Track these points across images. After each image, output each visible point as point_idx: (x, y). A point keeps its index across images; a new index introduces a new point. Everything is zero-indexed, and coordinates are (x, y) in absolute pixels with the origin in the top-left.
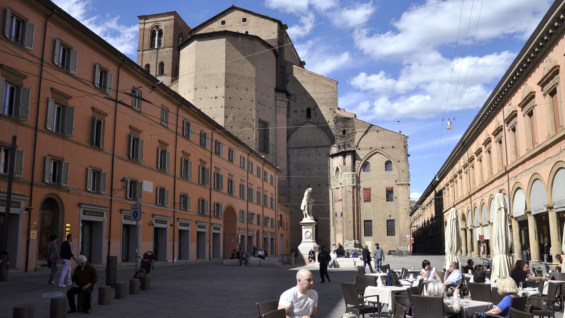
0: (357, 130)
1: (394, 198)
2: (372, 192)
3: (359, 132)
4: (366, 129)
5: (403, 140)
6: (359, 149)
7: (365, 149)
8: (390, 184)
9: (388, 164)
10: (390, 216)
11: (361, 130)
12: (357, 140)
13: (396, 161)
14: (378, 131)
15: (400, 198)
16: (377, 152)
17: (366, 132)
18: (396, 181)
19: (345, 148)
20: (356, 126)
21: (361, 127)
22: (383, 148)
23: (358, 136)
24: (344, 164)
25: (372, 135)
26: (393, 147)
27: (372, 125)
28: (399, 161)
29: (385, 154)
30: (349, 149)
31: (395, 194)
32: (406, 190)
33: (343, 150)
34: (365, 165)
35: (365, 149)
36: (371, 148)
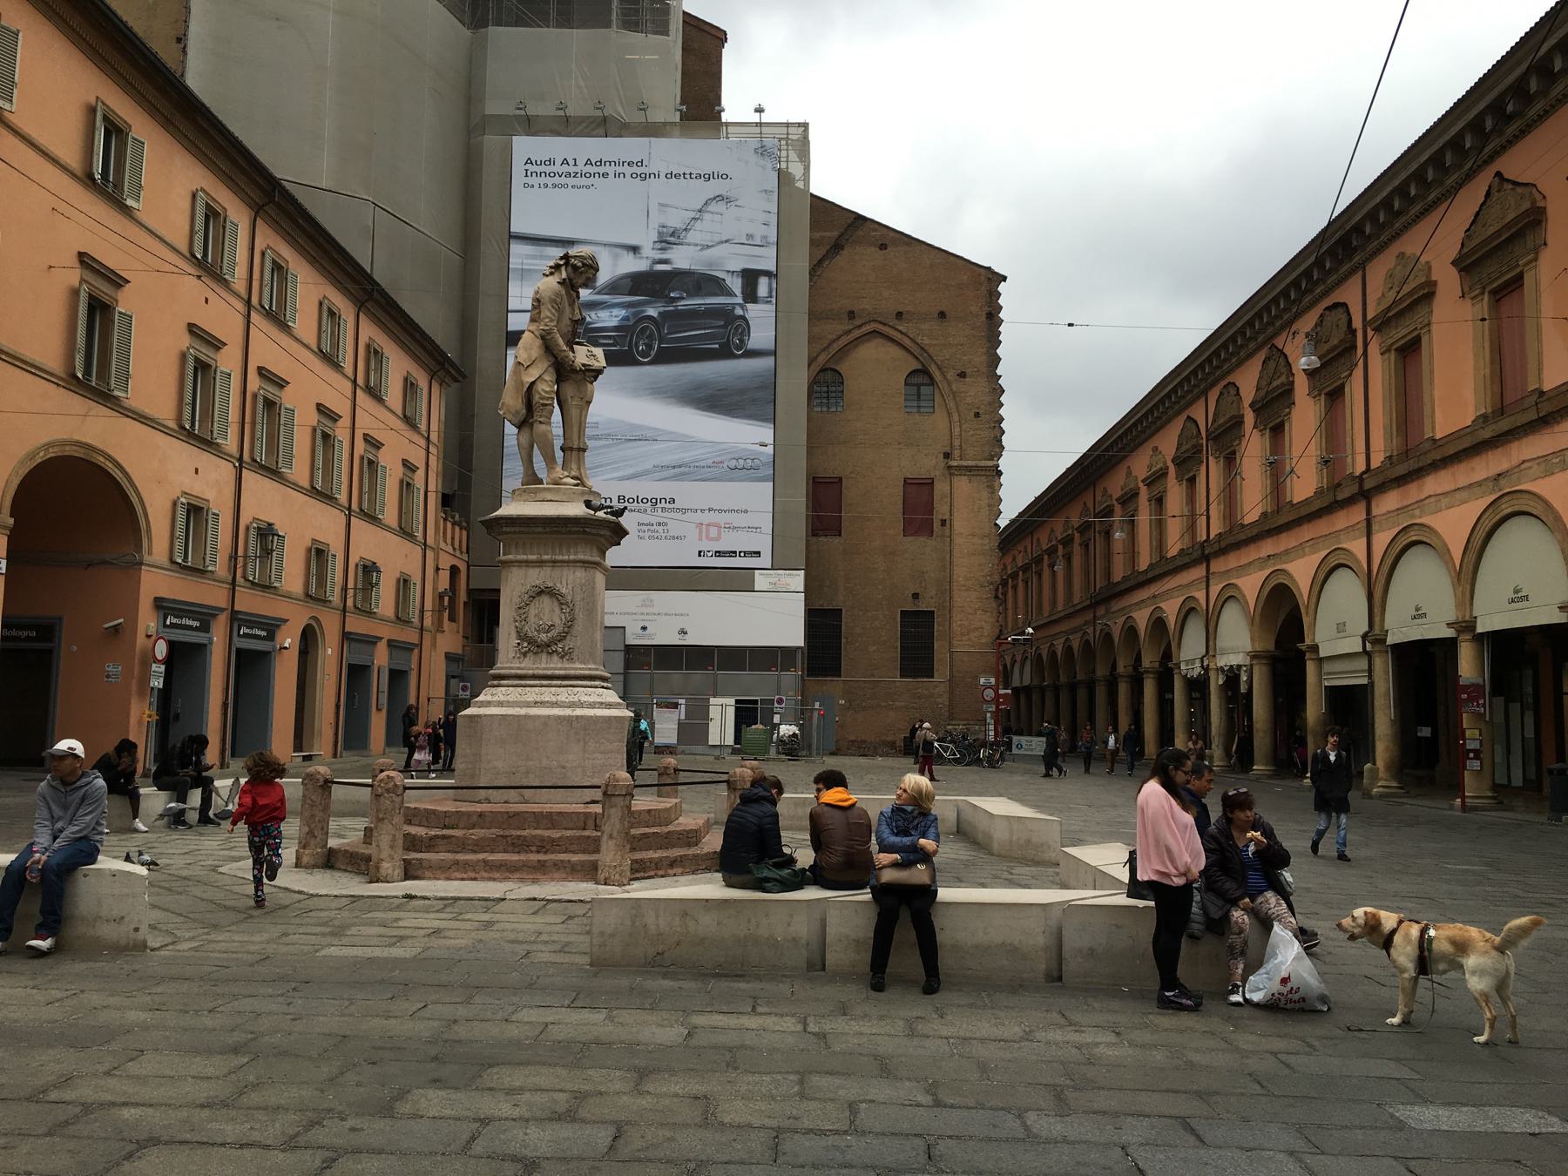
1: (937, 524)
2: (850, 493)
5: (984, 289)
8: (927, 464)
10: (916, 596)
13: (951, 375)
14: (883, 247)
15: (956, 524)
16: (875, 333)
18: (947, 456)
22: (899, 315)
26: (942, 315)
28: (962, 375)
29: (907, 342)
31: (941, 510)
32: (985, 494)
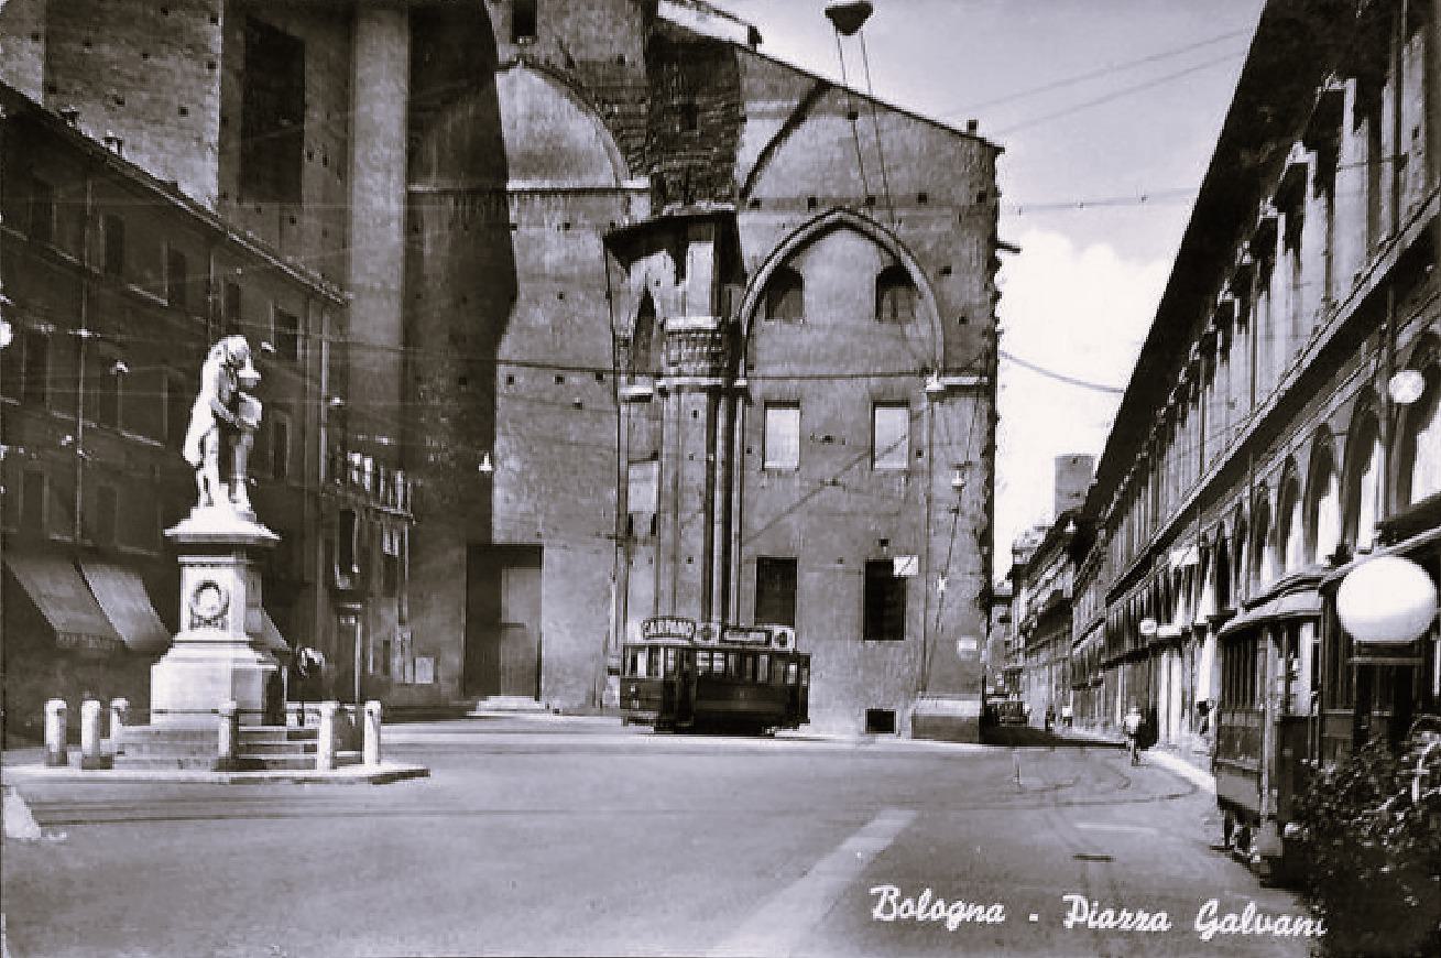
0: (751, 107)
3: (761, 115)
4: (796, 103)
6: (756, 204)
7: (780, 205)
9: (893, 279)
11: (774, 106)
12: (747, 156)
17: (796, 119)
19: (689, 201)
20: (745, 83)
21: (774, 92)
22: (871, 201)
23: (755, 136)
24: (680, 273)
25: (823, 132)
27: (823, 86)
29: (881, 235)
30: (704, 206)
33: (675, 208)
34: (785, 283)
35: (780, 205)
36: (812, 203)
